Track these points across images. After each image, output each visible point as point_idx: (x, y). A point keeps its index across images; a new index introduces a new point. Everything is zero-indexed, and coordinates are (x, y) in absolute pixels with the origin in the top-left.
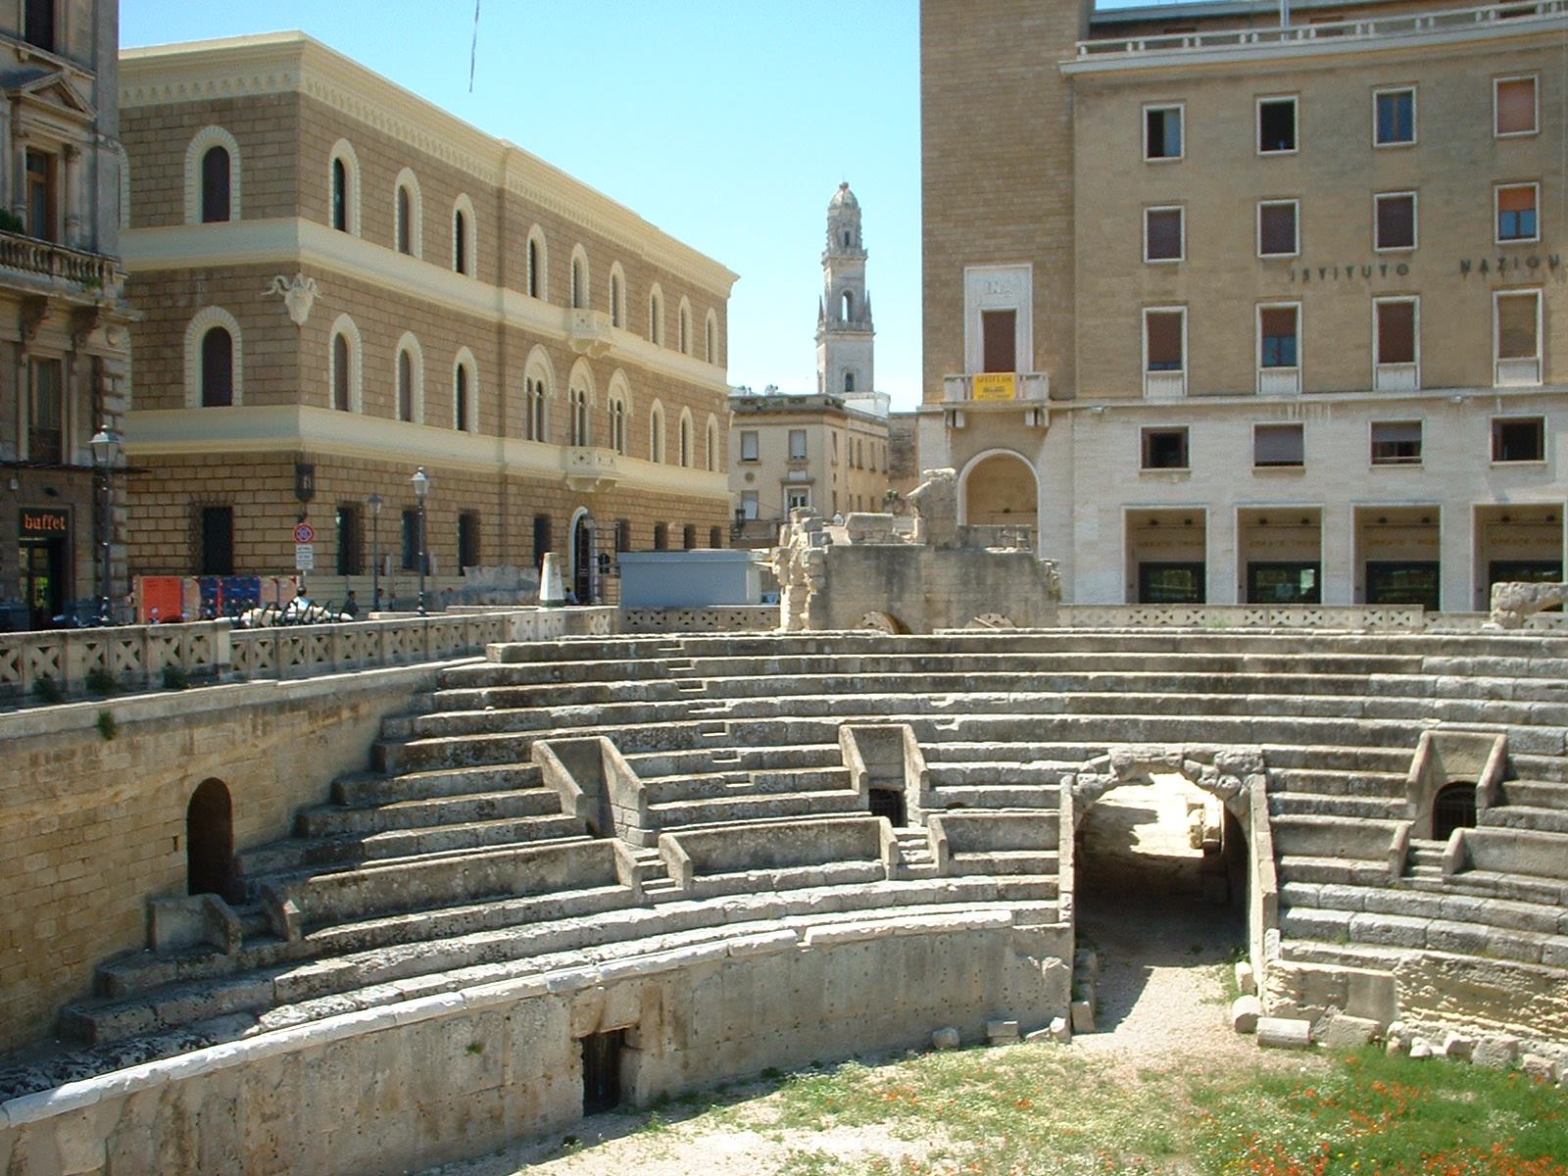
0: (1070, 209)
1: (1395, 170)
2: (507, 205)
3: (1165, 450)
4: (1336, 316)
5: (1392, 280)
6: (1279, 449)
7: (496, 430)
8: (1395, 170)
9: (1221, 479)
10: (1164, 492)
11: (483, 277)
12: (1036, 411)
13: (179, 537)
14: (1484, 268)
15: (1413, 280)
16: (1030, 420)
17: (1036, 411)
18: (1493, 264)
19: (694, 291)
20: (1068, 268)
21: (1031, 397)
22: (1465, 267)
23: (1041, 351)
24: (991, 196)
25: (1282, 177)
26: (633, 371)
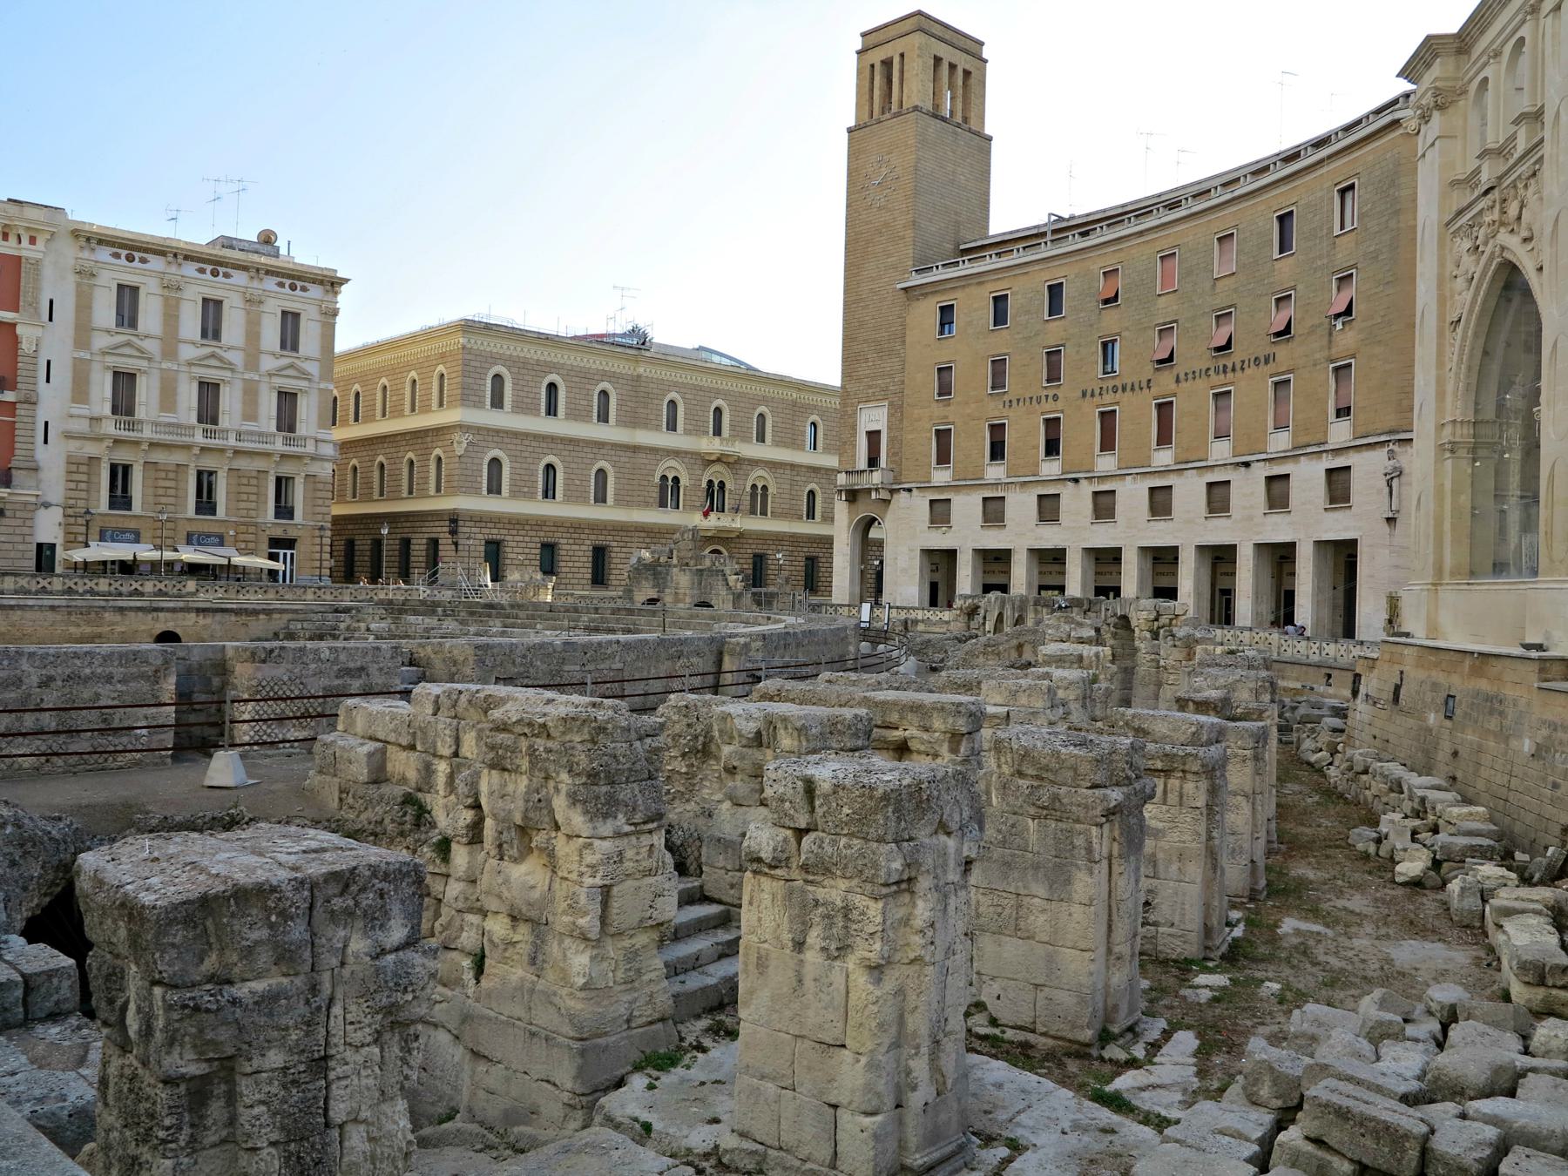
1: (1055, 332)
3: (940, 512)
4: (1025, 433)
5: (1050, 405)
6: (993, 511)
8: (1055, 332)
9: (967, 533)
10: (940, 540)
11: (621, 423)
12: (877, 490)
14: (1092, 395)
15: (1060, 405)
17: (877, 490)
18: (1097, 392)
20: (901, 406)
22: (1084, 394)
25: (1001, 342)
26: (773, 465)
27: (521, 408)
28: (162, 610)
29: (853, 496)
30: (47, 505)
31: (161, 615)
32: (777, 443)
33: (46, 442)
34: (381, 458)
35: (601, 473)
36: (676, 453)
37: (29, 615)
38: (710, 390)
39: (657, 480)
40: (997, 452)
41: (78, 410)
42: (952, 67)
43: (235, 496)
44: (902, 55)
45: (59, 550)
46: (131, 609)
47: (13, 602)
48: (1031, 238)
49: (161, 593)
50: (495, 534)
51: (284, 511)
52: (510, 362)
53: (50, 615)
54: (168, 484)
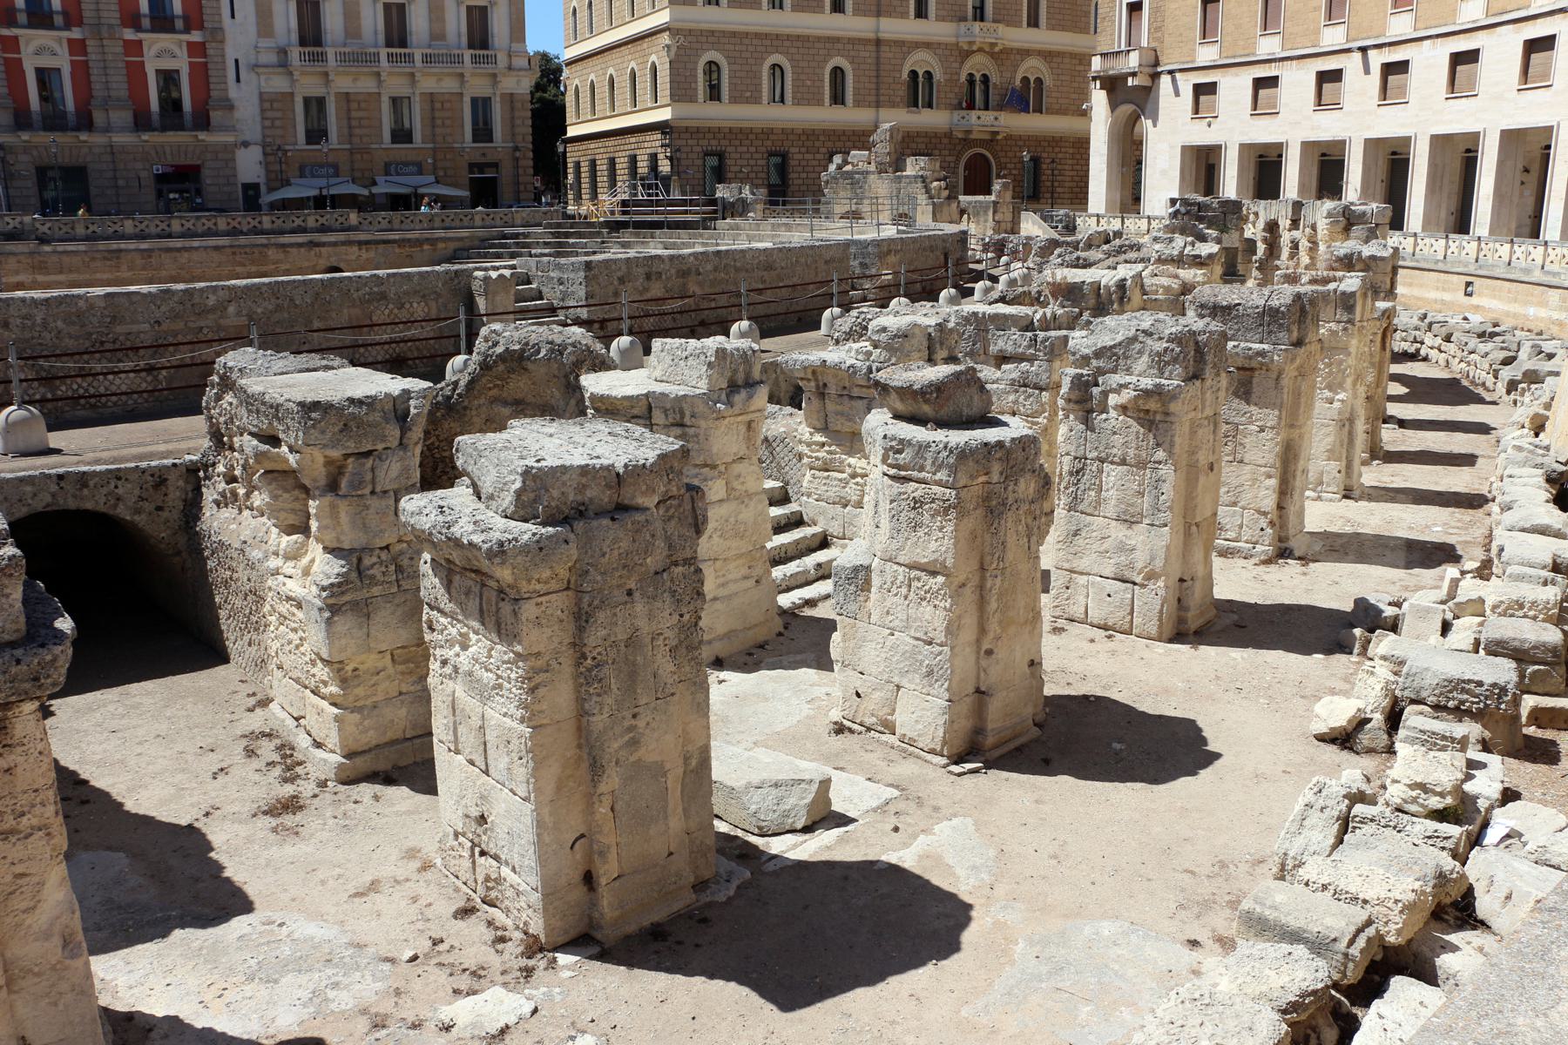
12: (1134, 74)
16: (1130, 82)
26: (1048, 55)
28: (323, 244)
29: (1113, 84)
30: (246, 144)
31: (323, 250)
32: (1051, 27)
33: (238, 80)
34: (611, 71)
36: (927, 45)
37: (195, 256)
39: (905, 75)
41: (265, 43)
43: (431, 121)
45: (263, 188)
46: (292, 245)
47: (179, 245)
49: (323, 229)
50: (714, 145)
51: (483, 132)
53: (215, 255)
54: (360, 114)
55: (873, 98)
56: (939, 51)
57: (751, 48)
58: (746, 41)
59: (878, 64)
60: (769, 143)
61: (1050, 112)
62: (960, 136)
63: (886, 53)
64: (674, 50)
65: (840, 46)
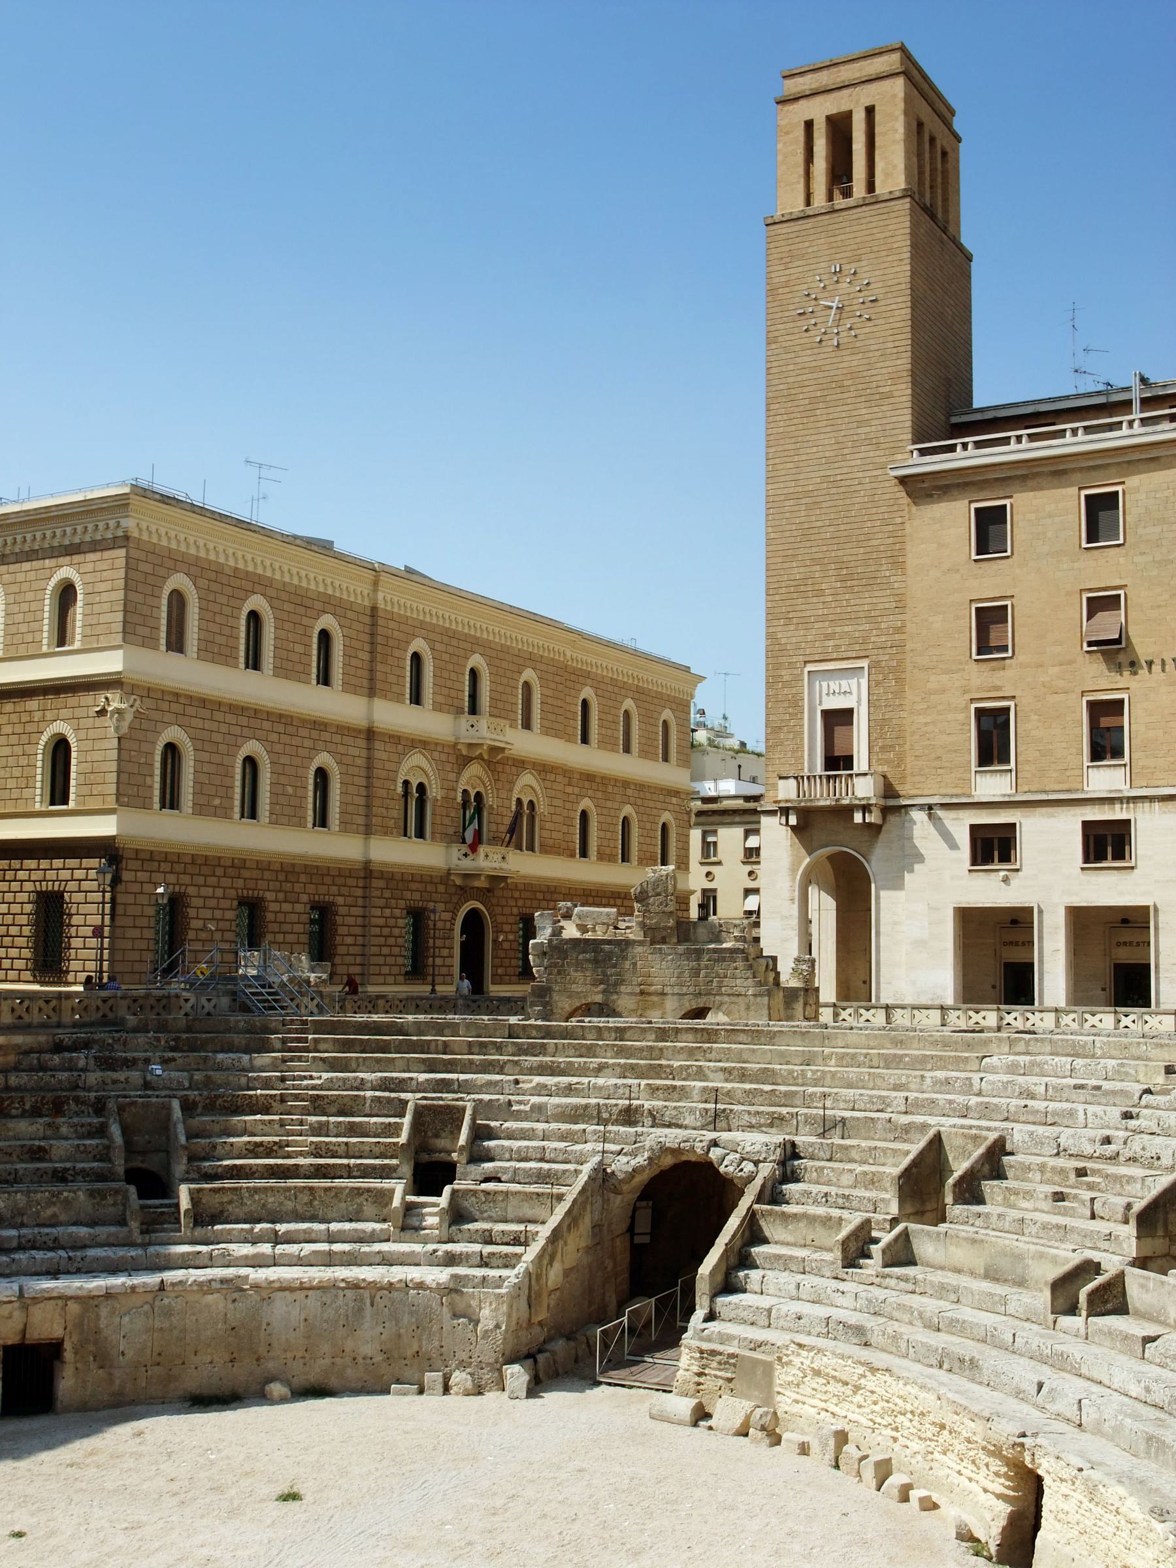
0: (901, 607)
2: (381, 622)
3: (993, 846)
7: (362, 828)
10: (991, 890)
11: (349, 687)
12: (866, 809)
13: (23, 920)
16: (858, 818)
19: (640, 694)
21: (860, 793)
23: (877, 749)
24: (830, 598)
26: (544, 769)
27: (214, 652)
32: (547, 731)
35: (322, 775)
36: (422, 744)
38: (466, 638)
39: (400, 789)
40: (1105, 745)
42: (932, 140)
44: (870, 111)
48: (1038, 418)
52: (198, 568)
55: (360, 820)
56: (436, 755)
57: (224, 728)
58: (219, 716)
59: (369, 768)
60: (240, 883)
61: (547, 850)
62: (458, 882)
63: (381, 752)
64: (129, 717)
65: (326, 736)
